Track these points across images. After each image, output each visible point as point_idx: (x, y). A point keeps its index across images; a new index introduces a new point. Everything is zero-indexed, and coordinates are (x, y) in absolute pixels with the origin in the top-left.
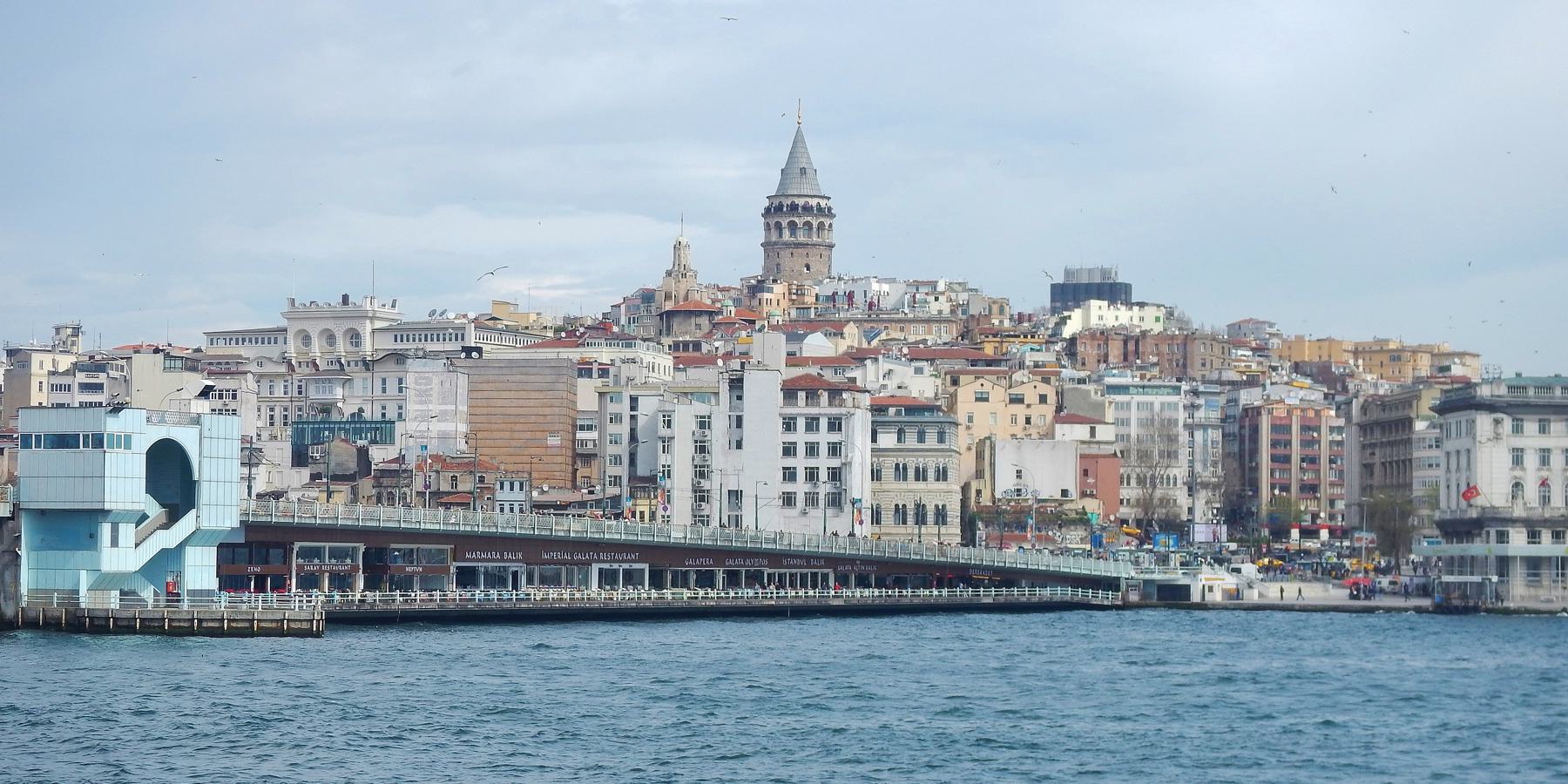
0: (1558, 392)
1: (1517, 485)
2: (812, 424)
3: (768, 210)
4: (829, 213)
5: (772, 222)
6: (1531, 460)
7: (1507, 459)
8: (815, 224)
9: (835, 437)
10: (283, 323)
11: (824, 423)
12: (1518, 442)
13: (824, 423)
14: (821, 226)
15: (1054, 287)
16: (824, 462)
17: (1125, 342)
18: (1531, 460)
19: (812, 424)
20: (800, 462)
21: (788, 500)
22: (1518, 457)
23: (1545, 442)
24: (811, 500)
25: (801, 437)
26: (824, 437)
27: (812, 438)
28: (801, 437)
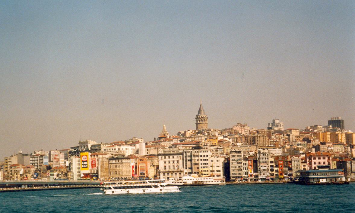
0: (171, 152)
1: (165, 166)
3: (196, 118)
6: (167, 162)
7: (164, 162)
8: (203, 119)
10: (78, 145)
12: (165, 160)
14: (204, 120)
15: (329, 121)
17: (245, 138)
18: (167, 162)
22: (165, 162)
23: (169, 160)
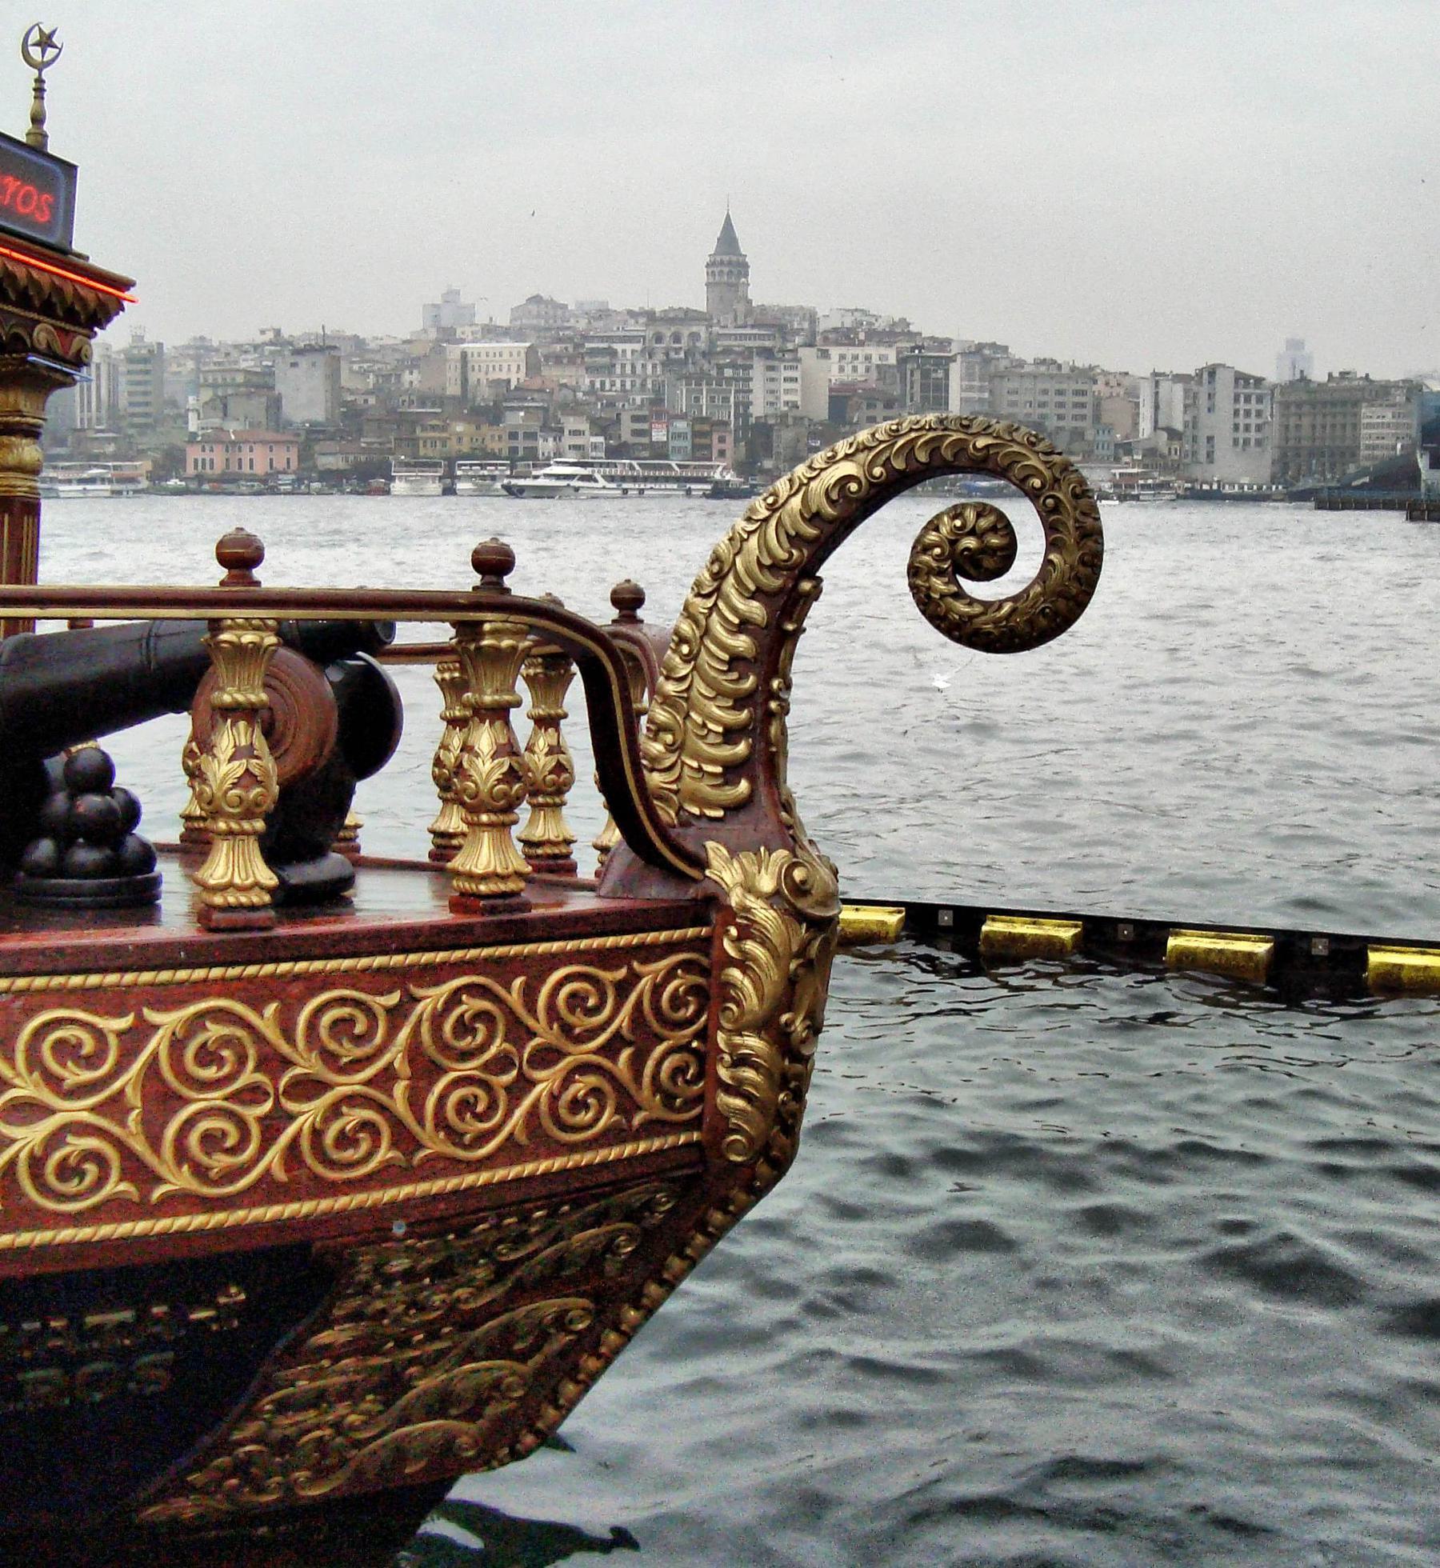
2: (1248, 399)
3: (708, 266)
4: (746, 266)
5: (716, 270)
9: (1260, 407)
11: (1253, 398)
13: (1253, 398)
16: (1253, 421)
19: (1248, 399)
20: (1241, 421)
21: (1236, 442)
24: (1246, 442)
25: (1242, 406)
26: (1253, 406)
27: (1248, 407)
28: (1242, 406)
